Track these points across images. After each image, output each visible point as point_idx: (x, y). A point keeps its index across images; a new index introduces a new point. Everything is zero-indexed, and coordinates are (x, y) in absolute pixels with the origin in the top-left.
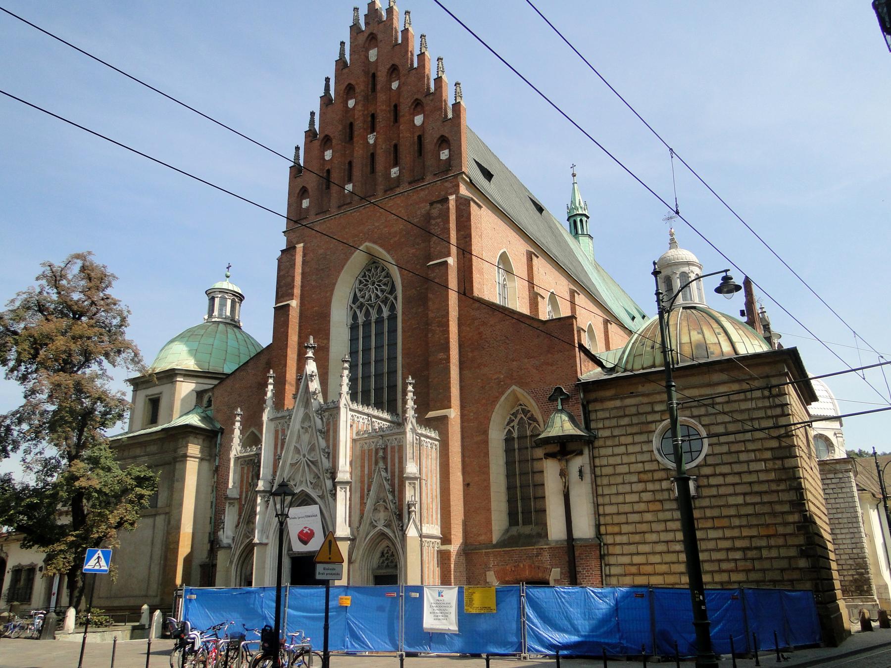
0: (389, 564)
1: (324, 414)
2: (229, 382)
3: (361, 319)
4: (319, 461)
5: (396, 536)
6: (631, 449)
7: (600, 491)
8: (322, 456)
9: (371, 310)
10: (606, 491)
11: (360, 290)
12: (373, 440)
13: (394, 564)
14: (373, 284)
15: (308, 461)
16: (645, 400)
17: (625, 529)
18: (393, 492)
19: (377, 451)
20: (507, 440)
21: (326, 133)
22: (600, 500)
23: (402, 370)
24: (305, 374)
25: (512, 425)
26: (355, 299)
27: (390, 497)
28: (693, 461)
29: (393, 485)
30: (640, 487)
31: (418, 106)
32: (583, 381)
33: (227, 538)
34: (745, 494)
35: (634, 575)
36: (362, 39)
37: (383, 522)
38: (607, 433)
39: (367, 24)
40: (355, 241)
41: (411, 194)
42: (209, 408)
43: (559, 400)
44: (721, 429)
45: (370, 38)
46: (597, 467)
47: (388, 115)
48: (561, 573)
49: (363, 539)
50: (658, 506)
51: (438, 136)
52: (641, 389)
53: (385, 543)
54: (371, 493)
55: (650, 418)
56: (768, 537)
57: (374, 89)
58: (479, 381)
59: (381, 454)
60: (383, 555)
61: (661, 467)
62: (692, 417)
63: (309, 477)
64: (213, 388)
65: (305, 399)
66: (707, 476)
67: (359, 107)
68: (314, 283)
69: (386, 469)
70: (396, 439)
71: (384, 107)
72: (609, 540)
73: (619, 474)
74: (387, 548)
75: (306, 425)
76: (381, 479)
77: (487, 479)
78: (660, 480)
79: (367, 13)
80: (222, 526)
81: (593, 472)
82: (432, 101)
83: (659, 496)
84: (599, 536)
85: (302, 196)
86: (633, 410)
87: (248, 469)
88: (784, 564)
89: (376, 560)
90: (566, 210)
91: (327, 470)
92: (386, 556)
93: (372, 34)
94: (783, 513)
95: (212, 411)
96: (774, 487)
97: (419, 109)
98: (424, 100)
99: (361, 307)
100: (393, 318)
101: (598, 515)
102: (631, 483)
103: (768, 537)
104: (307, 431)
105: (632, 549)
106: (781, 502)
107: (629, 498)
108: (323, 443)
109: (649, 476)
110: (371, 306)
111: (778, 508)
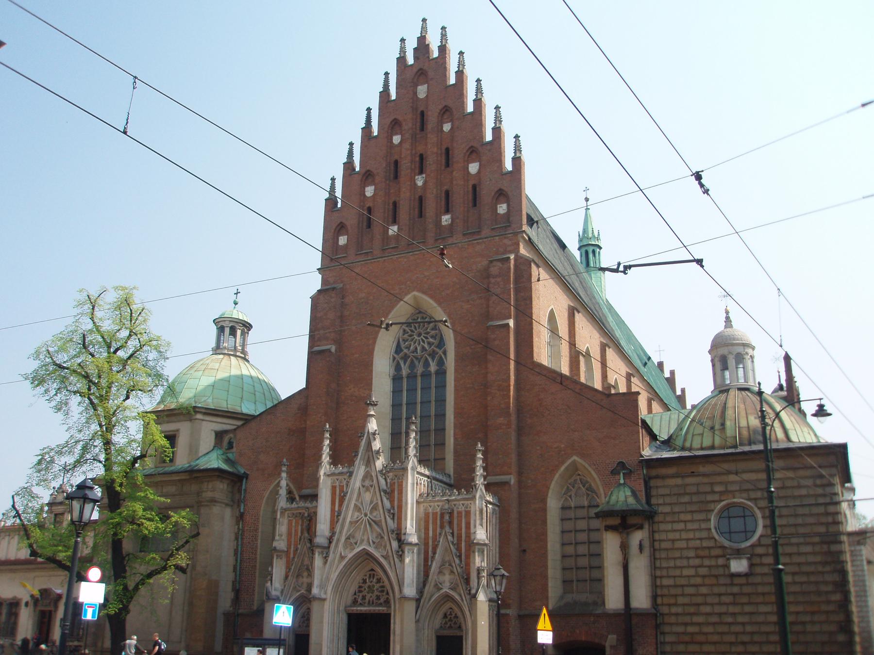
0: (452, 625)
1: (389, 475)
2: (253, 424)
3: (405, 371)
6: (690, 526)
7: (658, 564)
8: (387, 517)
9: (416, 362)
10: (664, 564)
11: (403, 340)
12: (439, 503)
13: (458, 625)
14: (419, 335)
15: (370, 520)
17: (681, 600)
18: (460, 557)
19: (442, 515)
21: (368, 169)
22: (658, 573)
23: (454, 431)
24: (366, 431)
25: (569, 494)
26: (398, 350)
27: (457, 561)
28: (747, 540)
29: (459, 549)
30: (697, 562)
32: (646, 458)
33: (275, 590)
35: (687, 643)
37: (448, 584)
38: (667, 509)
39: (416, 58)
40: (401, 289)
41: (466, 246)
42: (231, 451)
43: (622, 474)
45: (418, 74)
47: (439, 159)
48: (618, 640)
49: (427, 600)
50: (713, 581)
51: (496, 189)
52: (702, 469)
53: (449, 605)
55: (709, 498)
57: (422, 128)
58: (538, 448)
59: (447, 517)
60: (445, 616)
61: (718, 545)
62: (749, 499)
64: (235, 430)
65: (366, 457)
66: (761, 556)
67: (407, 145)
69: (453, 534)
70: (463, 505)
71: (435, 150)
72: (665, 610)
73: (677, 549)
74: (451, 610)
76: (447, 543)
77: (545, 547)
78: (717, 557)
80: (269, 577)
81: (652, 546)
82: (489, 150)
83: (714, 572)
84: (656, 607)
85: (339, 231)
86: (694, 489)
87: (297, 522)
89: (438, 621)
90: (577, 239)
91: (393, 531)
92: (449, 617)
93: (421, 69)
94: (827, 593)
95: (234, 454)
96: (820, 568)
97: (474, 156)
99: (405, 358)
100: (441, 373)
102: (688, 558)
104: (367, 489)
105: (687, 619)
106: (826, 583)
107: (686, 572)
109: (706, 553)
110: (417, 358)
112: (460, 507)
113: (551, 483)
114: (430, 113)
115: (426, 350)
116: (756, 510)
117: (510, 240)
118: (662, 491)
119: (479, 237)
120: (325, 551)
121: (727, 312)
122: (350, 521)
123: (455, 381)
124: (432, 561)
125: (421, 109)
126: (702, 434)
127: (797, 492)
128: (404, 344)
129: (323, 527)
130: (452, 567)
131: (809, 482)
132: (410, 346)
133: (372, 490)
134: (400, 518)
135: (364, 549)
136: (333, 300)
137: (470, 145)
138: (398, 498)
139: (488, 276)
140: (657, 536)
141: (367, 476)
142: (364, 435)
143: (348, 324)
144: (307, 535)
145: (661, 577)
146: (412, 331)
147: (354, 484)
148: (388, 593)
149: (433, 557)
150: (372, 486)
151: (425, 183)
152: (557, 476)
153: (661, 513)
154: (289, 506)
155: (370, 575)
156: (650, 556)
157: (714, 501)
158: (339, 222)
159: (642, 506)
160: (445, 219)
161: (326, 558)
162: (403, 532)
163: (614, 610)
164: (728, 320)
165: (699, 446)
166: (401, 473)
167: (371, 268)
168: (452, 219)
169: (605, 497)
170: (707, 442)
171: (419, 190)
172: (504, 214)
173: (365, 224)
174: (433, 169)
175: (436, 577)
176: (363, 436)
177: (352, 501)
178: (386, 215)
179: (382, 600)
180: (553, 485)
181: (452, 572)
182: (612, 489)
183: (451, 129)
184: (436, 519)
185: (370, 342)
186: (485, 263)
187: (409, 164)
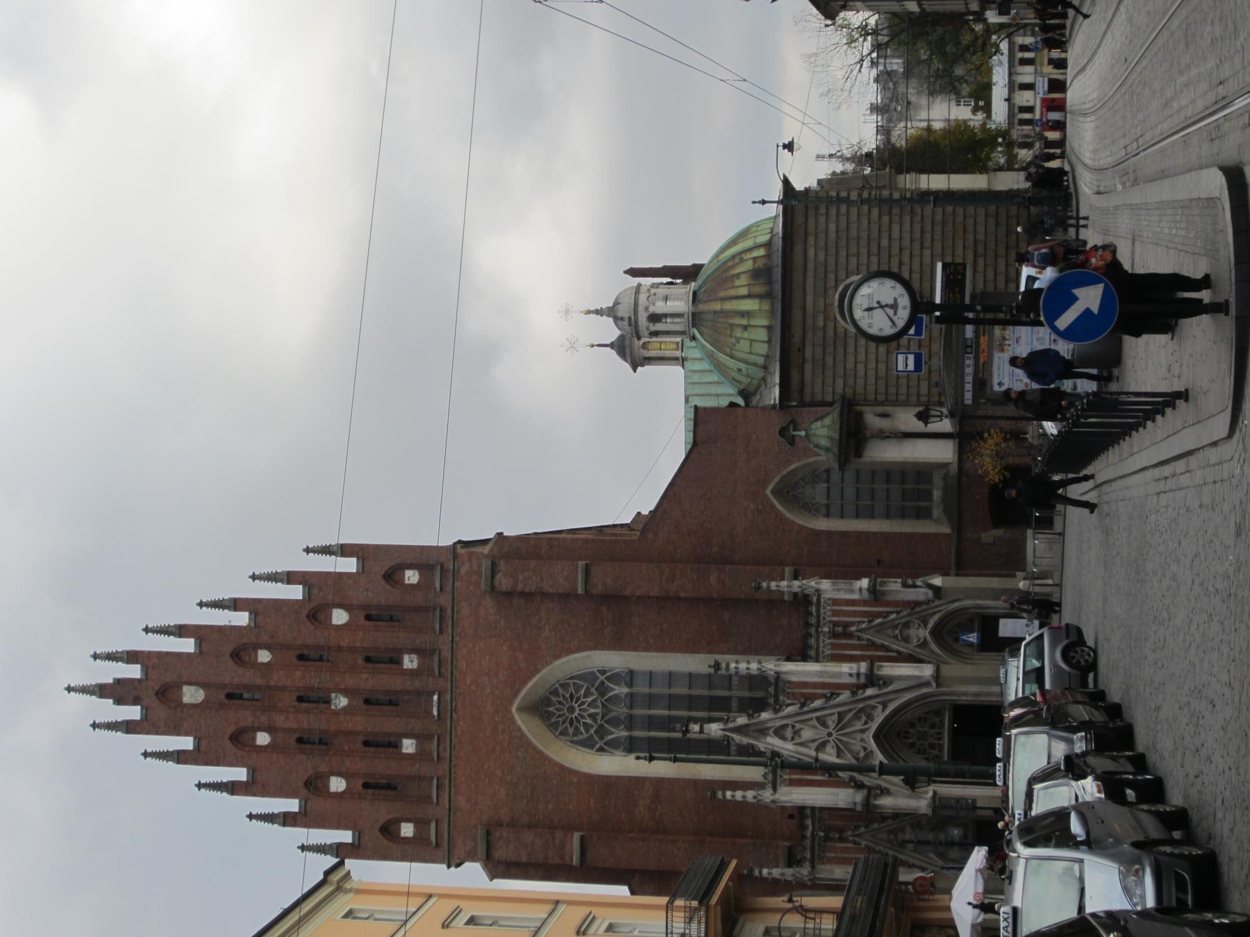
4: (839, 709)
5: (936, 612)
6: (861, 357)
10: (904, 390)
11: (575, 735)
12: (821, 640)
14: (572, 710)
16: (809, 336)
18: (888, 613)
19: (834, 635)
21: (301, 784)
22: (914, 398)
26: (588, 744)
27: (893, 616)
29: (879, 615)
32: (777, 402)
34: (922, 247)
36: (160, 712)
37: (921, 630)
38: (840, 383)
40: (504, 731)
44: (853, 261)
46: (876, 398)
47: (313, 669)
51: (384, 582)
52: (797, 339)
54: (886, 643)
55: (831, 332)
56: (965, 231)
58: (751, 538)
59: (840, 629)
62: (836, 287)
63: (858, 726)
65: (755, 734)
67: (280, 720)
68: (550, 807)
69: (859, 623)
71: (298, 673)
79: (111, 701)
81: (882, 404)
82: (320, 589)
86: (819, 350)
88: (992, 222)
96: (918, 219)
98: (314, 604)
99: (601, 732)
100: (630, 677)
103: (965, 231)
104: (797, 733)
106: (933, 214)
108: (818, 703)
111: (939, 218)
112: (828, 613)
113: (797, 524)
114: (236, 681)
115: (594, 701)
116: (848, 281)
117: (463, 564)
119: (449, 611)
120: (873, 792)
121: (589, 312)
122: (837, 757)
123: (649, 651)
124: (892, 651)
125: (222, 697)
126: (752, 341)
127: (832, 236)
128: (581, 734)
130: (899, 624)
131: (822, 219)
132: (585, 724)
133: (798, 726)
135: (873, 737)
136: (505, 834)
137: (306, 619)
138: (812, 688)
139: (509, 594)
140: (871, 397)
141: (779, 732)
142: (726, 735)
143: (542, 817)
144: (849, 833)
145: (918, 395)
146: (564, 722)
147: (788, 750)
148: (928, 713)
149: (887, 649)
150: (793, 727)
151: (346, 692)
152: (788, 515)
153: (844, 389)
154: (808, 863)
155: (907, 738)
156: (894, 406)
157: (835, 327)
158: (379, 834)
160: (410, 664)
162: (854, 680)
163: (954, 452)
164: (599, 312)
165: (766, 345)
166: (781, 683)
167: (462, 779)
168: (411, 651)
169: (820, 455)
170: (762, 335)
171: (354, 703)
172: (420, 575)
173: (389, 792)
174: (328, 678)
175: (911, 646)
176: (728, 736)
178: (383, 755)
179: (937, 720)
181: (907, 625)
182: (812, 446)
183: (269, 651)
184: (841, 644)
185: (575, 780)
186: (488, 602)
187: (312, 716)
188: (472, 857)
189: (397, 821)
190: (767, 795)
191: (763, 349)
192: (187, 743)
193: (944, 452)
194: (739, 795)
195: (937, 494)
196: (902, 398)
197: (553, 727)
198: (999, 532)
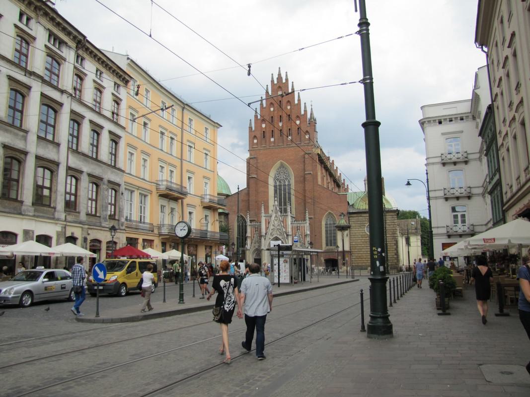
2: (230, 198)
3: (278, 183)
16: (364, 218)
17: (357, 248)
19: (297, 227)
20: (326, 224)
26: (275, 177)
30: (361, 238)
31: (298, 117)
36: (276, 87)
38: (354, 225)
39: (278, 82)
52: (363, 215)
55: (365, 222)
63: (278, 233)
67: (276, 112)
72: (353, 250)
75: (276, 219)
83: (366, 241)
97: (298, 118)
100: (289, 185)
101: (350, 244)
104: (276, 220)
108: (282, 224)
118: (352, 220)
129: (263, 231)
134: (286, 228)
139: (304, 157)
151: (282, 125)
159: (348, 225)
161: (265, 239)
173: (263, 136)
177: (272, 223)
180: (323, 218)
186: (303, 153)
188: (251, 155)
189: (257, 139)
190: (263, 214)
191: (361, 208)
192: (270, 93)
193: (340, 249)
194: (263, 209)
195: (331, 247)
196: (351, 239)
197: (278, 169)
198: (323, 261)
